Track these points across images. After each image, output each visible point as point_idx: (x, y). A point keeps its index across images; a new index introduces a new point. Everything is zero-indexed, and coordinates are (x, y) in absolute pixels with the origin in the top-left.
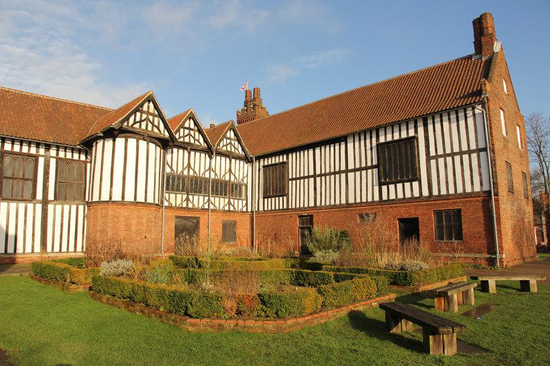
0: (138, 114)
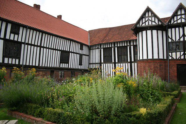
0: (144, 19)
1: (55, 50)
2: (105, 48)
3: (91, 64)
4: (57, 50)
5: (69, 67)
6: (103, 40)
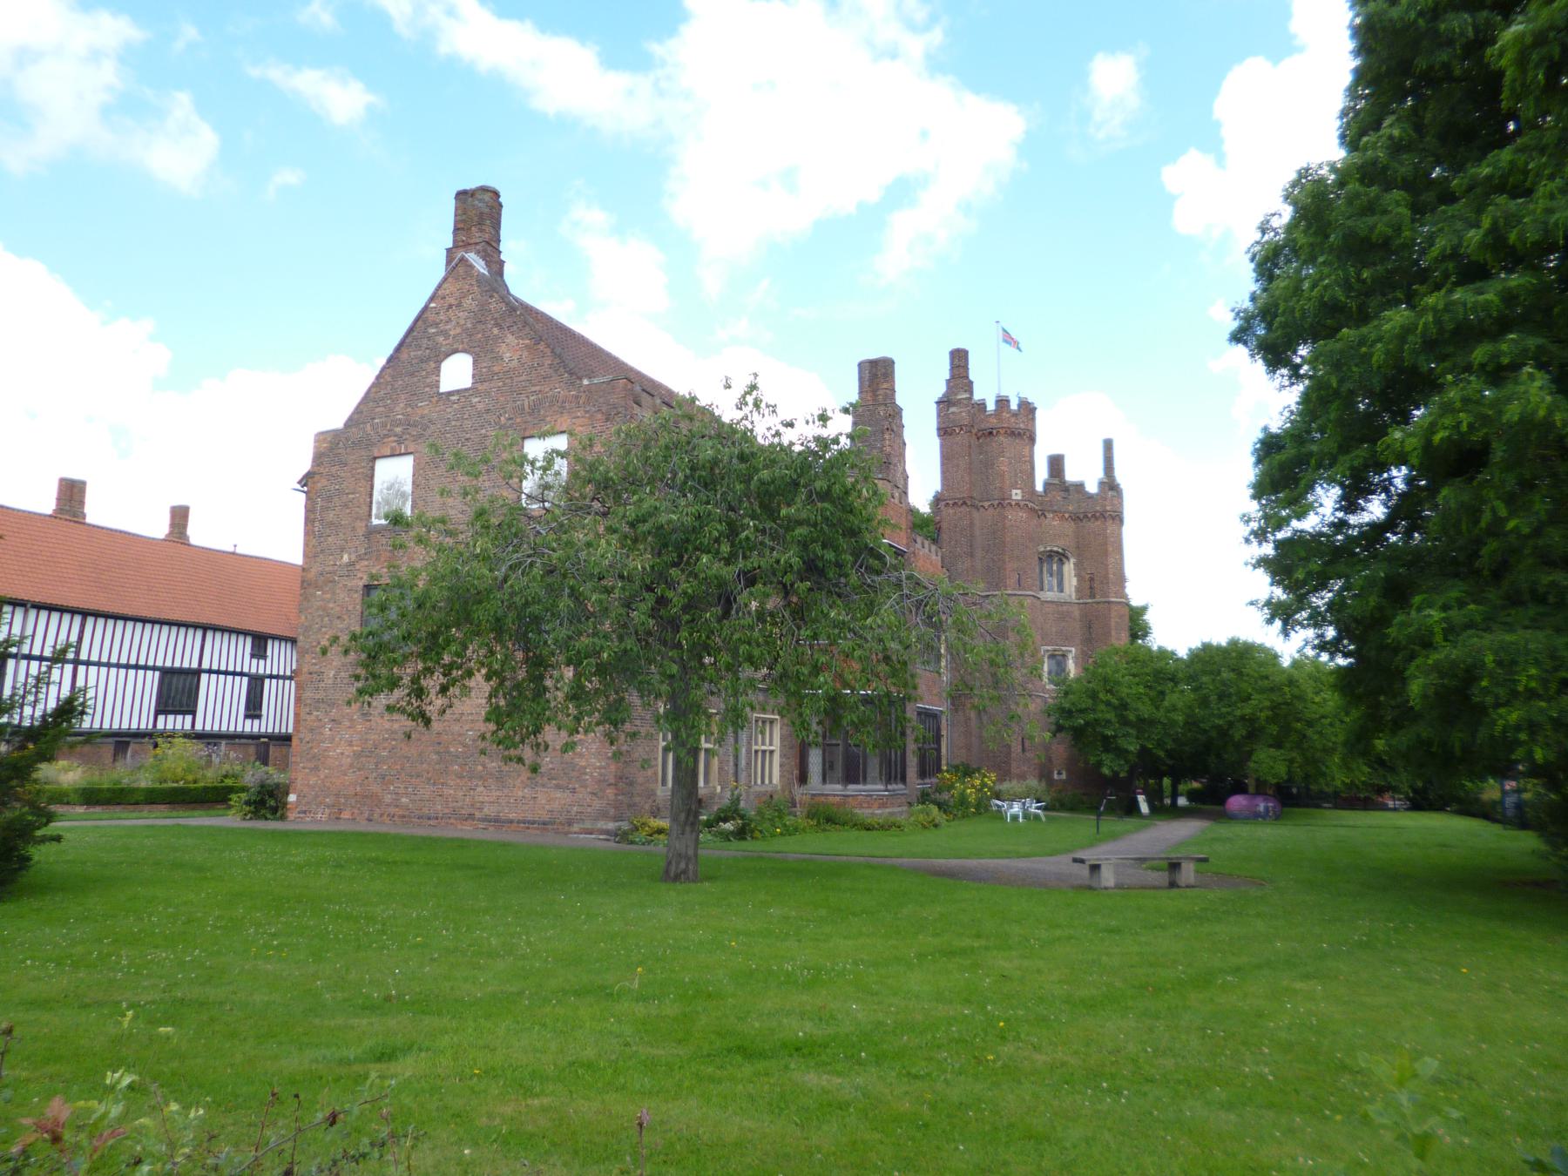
4: (146, 668)
5: (199, 727)
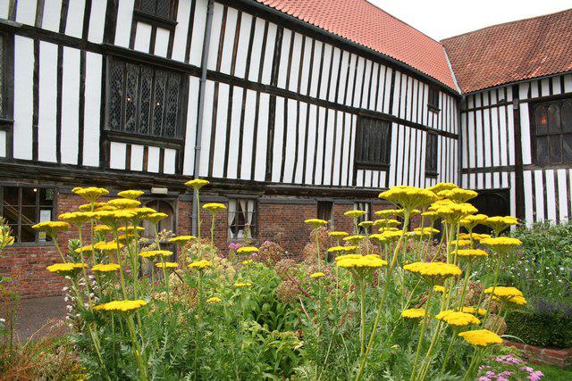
1: (336, 106)
2: (541, 100)
3: (468, 171)
4: (344, 109)
6: (524, 67)
